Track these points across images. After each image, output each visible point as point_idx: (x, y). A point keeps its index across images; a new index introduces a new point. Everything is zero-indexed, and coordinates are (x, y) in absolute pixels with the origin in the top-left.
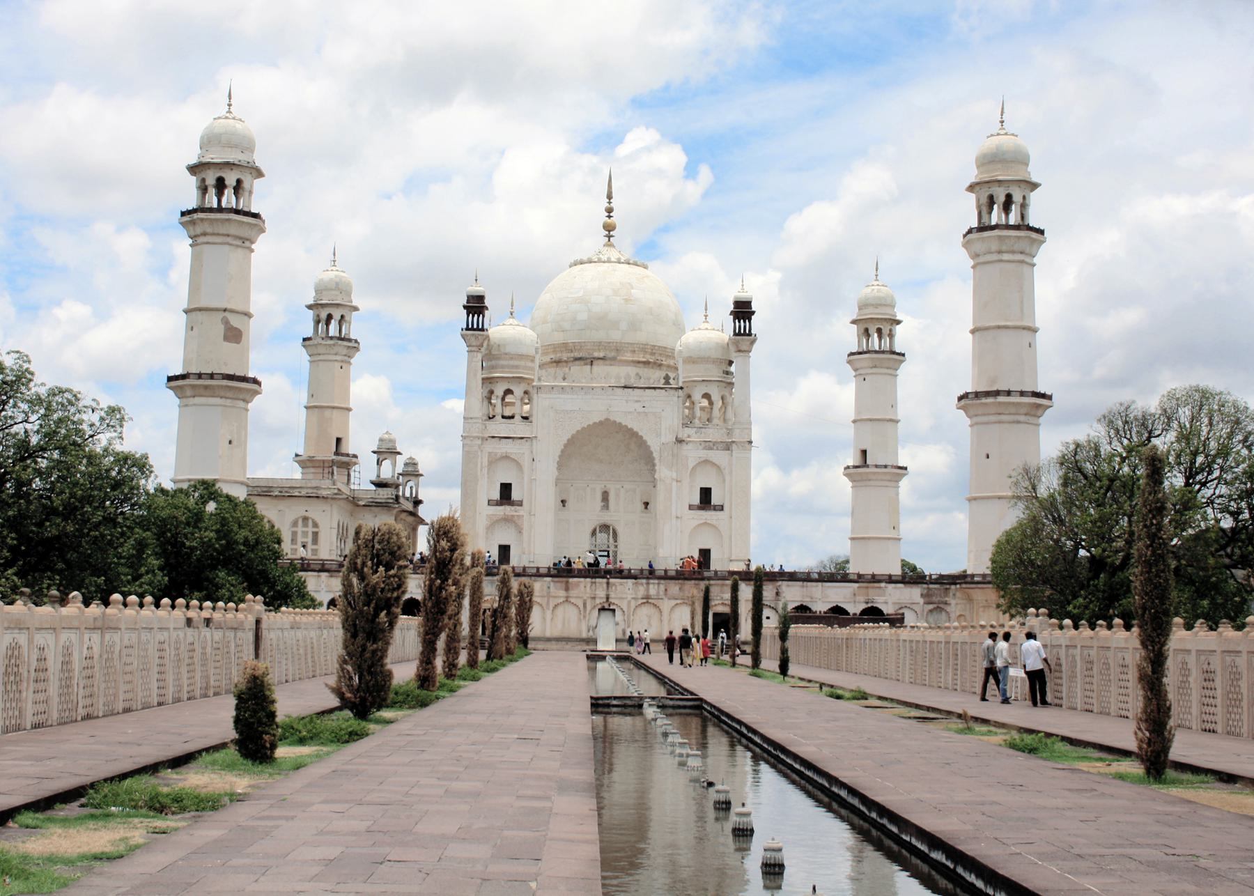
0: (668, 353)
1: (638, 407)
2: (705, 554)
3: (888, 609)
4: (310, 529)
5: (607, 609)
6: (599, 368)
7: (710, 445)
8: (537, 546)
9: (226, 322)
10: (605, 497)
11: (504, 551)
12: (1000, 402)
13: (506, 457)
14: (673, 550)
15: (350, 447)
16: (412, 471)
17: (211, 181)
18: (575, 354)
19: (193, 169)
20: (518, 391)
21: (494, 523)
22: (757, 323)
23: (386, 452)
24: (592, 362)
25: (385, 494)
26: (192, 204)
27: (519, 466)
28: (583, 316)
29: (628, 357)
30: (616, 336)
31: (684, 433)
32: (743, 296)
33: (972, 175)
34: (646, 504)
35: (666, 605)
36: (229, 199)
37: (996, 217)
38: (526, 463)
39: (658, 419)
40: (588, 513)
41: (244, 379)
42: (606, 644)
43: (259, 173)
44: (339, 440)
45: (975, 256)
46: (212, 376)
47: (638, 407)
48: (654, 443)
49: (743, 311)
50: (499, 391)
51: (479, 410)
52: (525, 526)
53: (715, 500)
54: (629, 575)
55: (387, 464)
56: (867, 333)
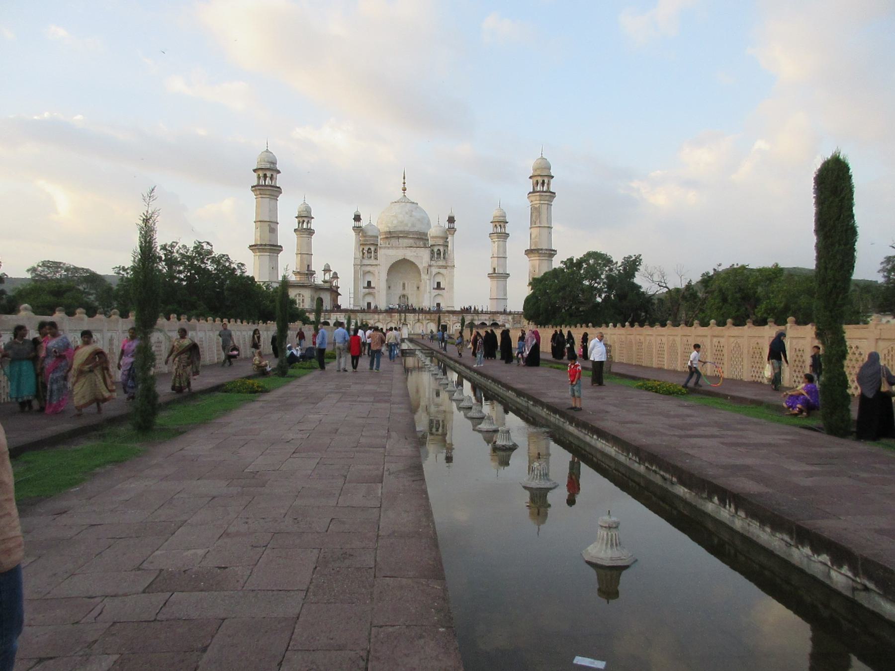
0: (426, 234)
3: (500, 323)
4: (301, 298)
7: (440, 267)
9: (269, 226)
10: (404, 285)
11: (369, 304)
14: (427, 302)
16: (335, 276)
18: (391, 235)
20: (373, 249)
22: (456, 225)
23: (327, 270)
24: (399, 237)
25: (327, 285)
28: (395, 222)
30: (407, 229)
32: (452, 215)
36: (268, 181)
37: (539, 188)
38: (376, 273)
39: (421, 258)
40: (399, 291)
41: (277, 246)
43: (279, 172)
46: (265, 245)
48: (420, 267)
50: (366, 248)
52: (377, 296)
53: (442, 286)
54: (414, 311)
55: (327, 274)
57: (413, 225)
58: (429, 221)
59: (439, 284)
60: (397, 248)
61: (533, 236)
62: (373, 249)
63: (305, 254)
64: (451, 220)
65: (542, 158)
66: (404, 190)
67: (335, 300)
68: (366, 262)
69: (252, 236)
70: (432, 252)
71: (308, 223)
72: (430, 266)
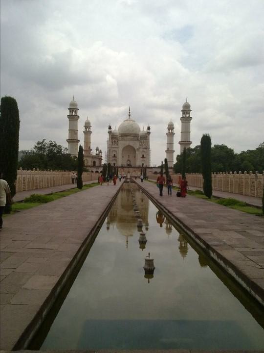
2: (143, 164)
5: (129, 172)
6: (128, 137)
8: (120, 162)
11: (114, 164)
12: (185, 143)
13: (114, 151)
14: (139, 163)
15: (91, 148)
16: (101, 152)
17: (71, 111)
18: (124, 135)
19: (69, 109)
22: (151, 131)
23: (97, 149)
24: (127, 136)
26: (69, 114)
27: (116, 152)
30: (131, 132)
31: (140, 147)
33: (182, 109)
34: (135, 157)
35: (137, 172)
39: (136, 145)
40: (126, 158)
42: (129, 177)
44: (89, 147)
48: (136, 148)
50: (113, 141)
51: (110, 143)
53: (145, 156)
57: (133, 131)
58: (140, 129)
59: (143, 155)
60: (126, 141)
63: (87, 142)
64: (149, 128)
65: (187, 103)
66: (129, 115)
67: (100, 162)
69: (66, 135)
71: (89, 128)
72: (140, 148)
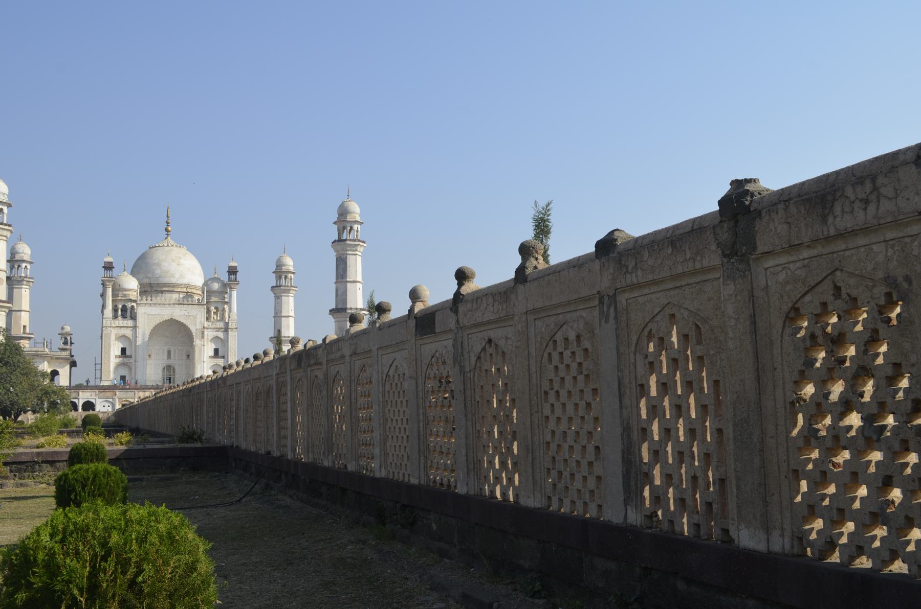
1: (186, 313)
6: (168, 295)
7: (218, 329)
10: (169, 352)
13: (124, 336)
21: (118, 366)
24: (162, 292)
29: (179, 290)
30: (173, 281)
39: (194, 317)
40: (162, 361)
45: (336, 251)
47: (186, 313)
49: (233, 271)
50: (120, 306)
53: (220, 354)
56: (280, 277)
61: (340, 293)
62: (129, 305)
68: (120, 322)
70: (209, 311)
